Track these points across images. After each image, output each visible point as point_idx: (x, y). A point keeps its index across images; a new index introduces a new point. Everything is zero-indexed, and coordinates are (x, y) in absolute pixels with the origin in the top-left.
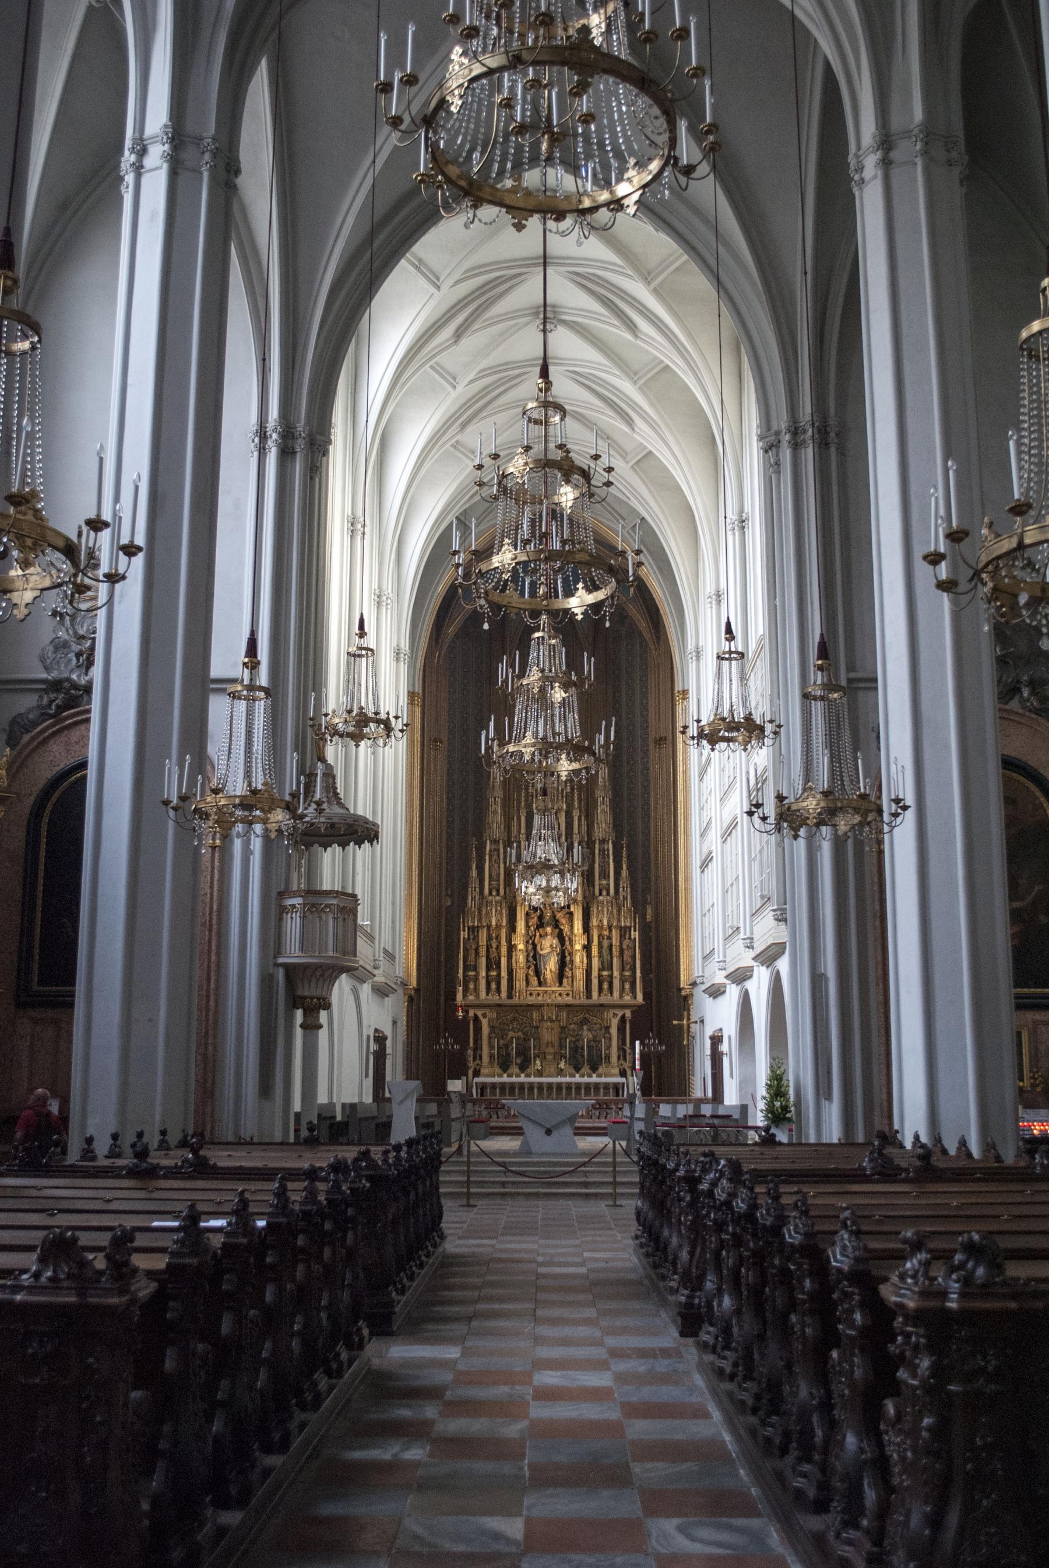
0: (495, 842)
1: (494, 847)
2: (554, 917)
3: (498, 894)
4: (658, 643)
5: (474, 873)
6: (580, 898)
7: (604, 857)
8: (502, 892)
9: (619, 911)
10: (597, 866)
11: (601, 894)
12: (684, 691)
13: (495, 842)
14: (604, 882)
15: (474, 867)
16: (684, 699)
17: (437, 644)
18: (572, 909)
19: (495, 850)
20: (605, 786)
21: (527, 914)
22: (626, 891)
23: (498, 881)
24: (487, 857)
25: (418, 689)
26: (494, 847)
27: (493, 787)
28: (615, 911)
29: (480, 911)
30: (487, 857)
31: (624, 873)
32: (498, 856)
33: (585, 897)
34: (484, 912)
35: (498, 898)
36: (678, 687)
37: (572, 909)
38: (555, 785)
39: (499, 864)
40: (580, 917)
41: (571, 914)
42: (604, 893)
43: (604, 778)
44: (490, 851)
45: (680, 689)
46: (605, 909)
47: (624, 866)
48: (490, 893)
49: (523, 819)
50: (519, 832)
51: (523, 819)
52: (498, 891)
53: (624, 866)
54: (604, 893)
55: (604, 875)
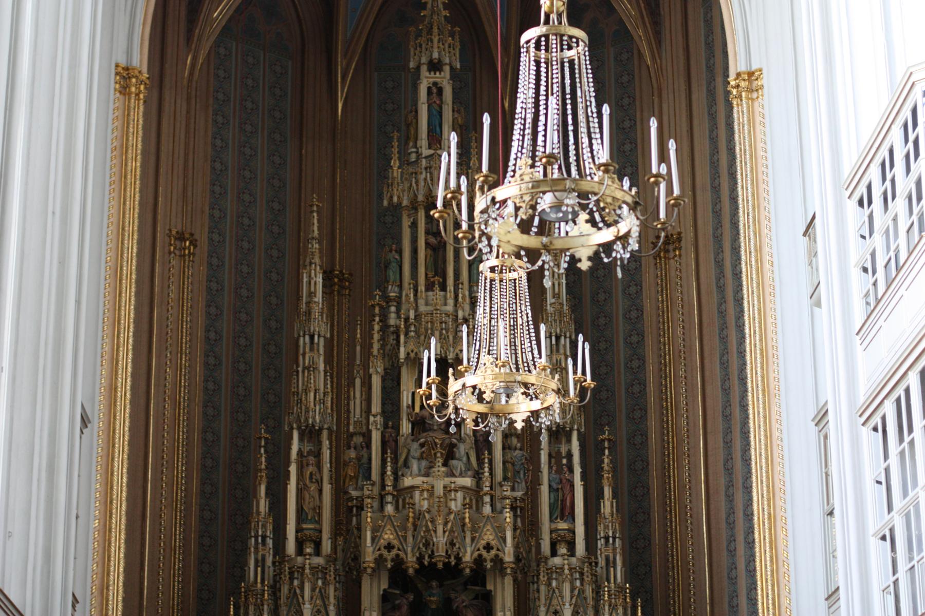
0: (311, 434)
1: (307, 448)
2: (448, 601)
3: (318, 552)
4: (659, 42)
5: (263, 505)
6: (508, 556)
7: (559, 471)
8: (327, 546)
9: (597, 592)
10: (545, 489)
11: (554, 553)
12: (751, 74)
13: (311, 434)
14: (563, 525)
15: (263, 489)
16: (750, 90)
17: (189, 40)
18: (490, 587)
19: (310, 453)
20: (561, 313)
21: (385, 598)
22: (613, 551)
23: (319, 522)
24: (293, 469)
25: (140, 60)
26: (307, 448)
27: (309, 313)
28: (589, 592)
29: (275, 590)
30: (293, 469)
31: (607, 507)
32: (319, 466)
33: (518, 559)
34: (285, 590)
35: (319, 561)
36: (737, 64)
37: (490, 587)
38: (450, 308)
39: (320, 482)
40: (509, 602)
41: (487, 599)
42: (563, 550)
43: (556, 296)
44: (300, 453)
45: (742, 68)
46: (567, 587)
47: (607, 492)
48: (300, 551)
49: (376, 381)
50: (368, 411)
51: (376, 381)
52: (318, 545)
53: (607, 492)
54: (563, 550)
55: (563, 510)
